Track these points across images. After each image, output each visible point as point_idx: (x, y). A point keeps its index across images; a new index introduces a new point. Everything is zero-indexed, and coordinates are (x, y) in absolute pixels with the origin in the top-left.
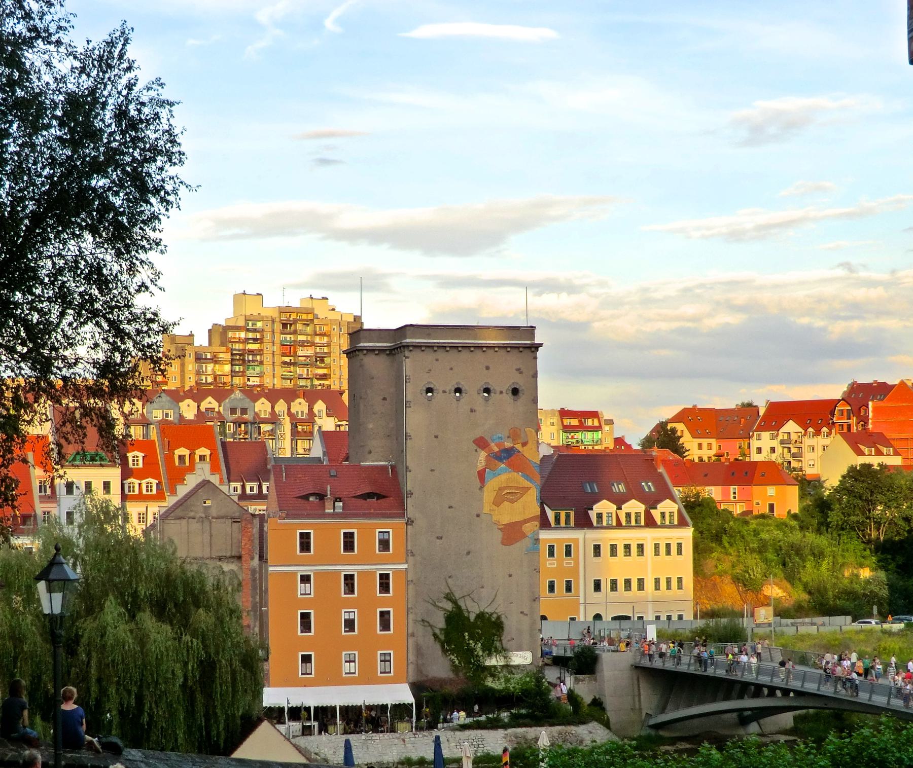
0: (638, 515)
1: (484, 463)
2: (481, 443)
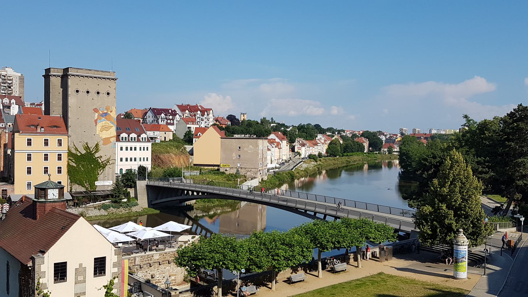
0: (135, 138)
1: (97, 117)
2: (96, 110)
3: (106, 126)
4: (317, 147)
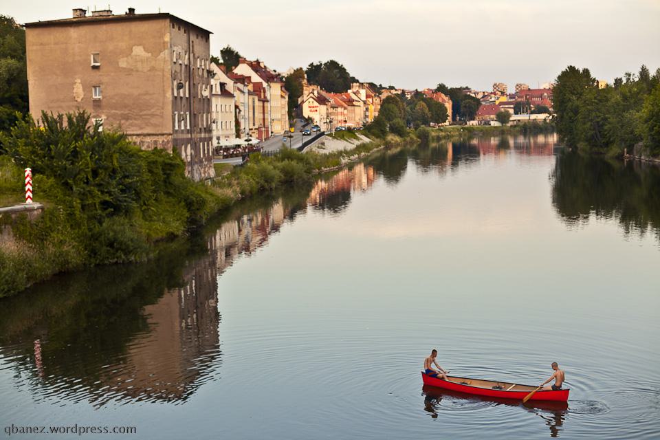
4: (353, 108)
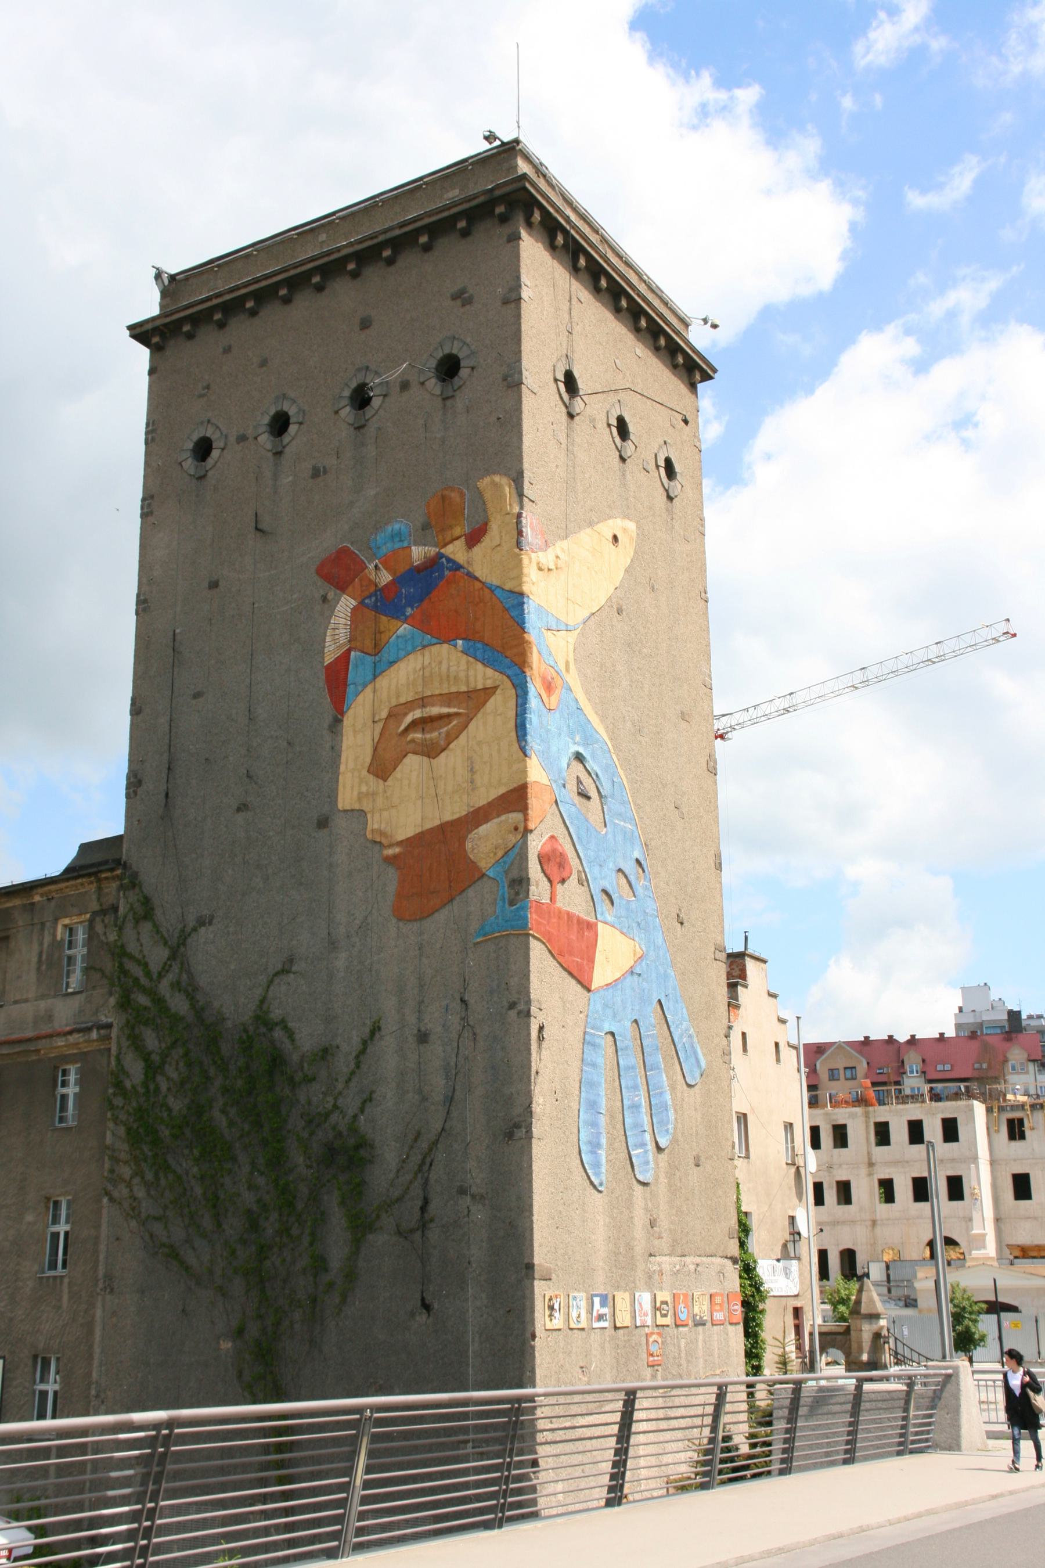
3: (423, 702)
